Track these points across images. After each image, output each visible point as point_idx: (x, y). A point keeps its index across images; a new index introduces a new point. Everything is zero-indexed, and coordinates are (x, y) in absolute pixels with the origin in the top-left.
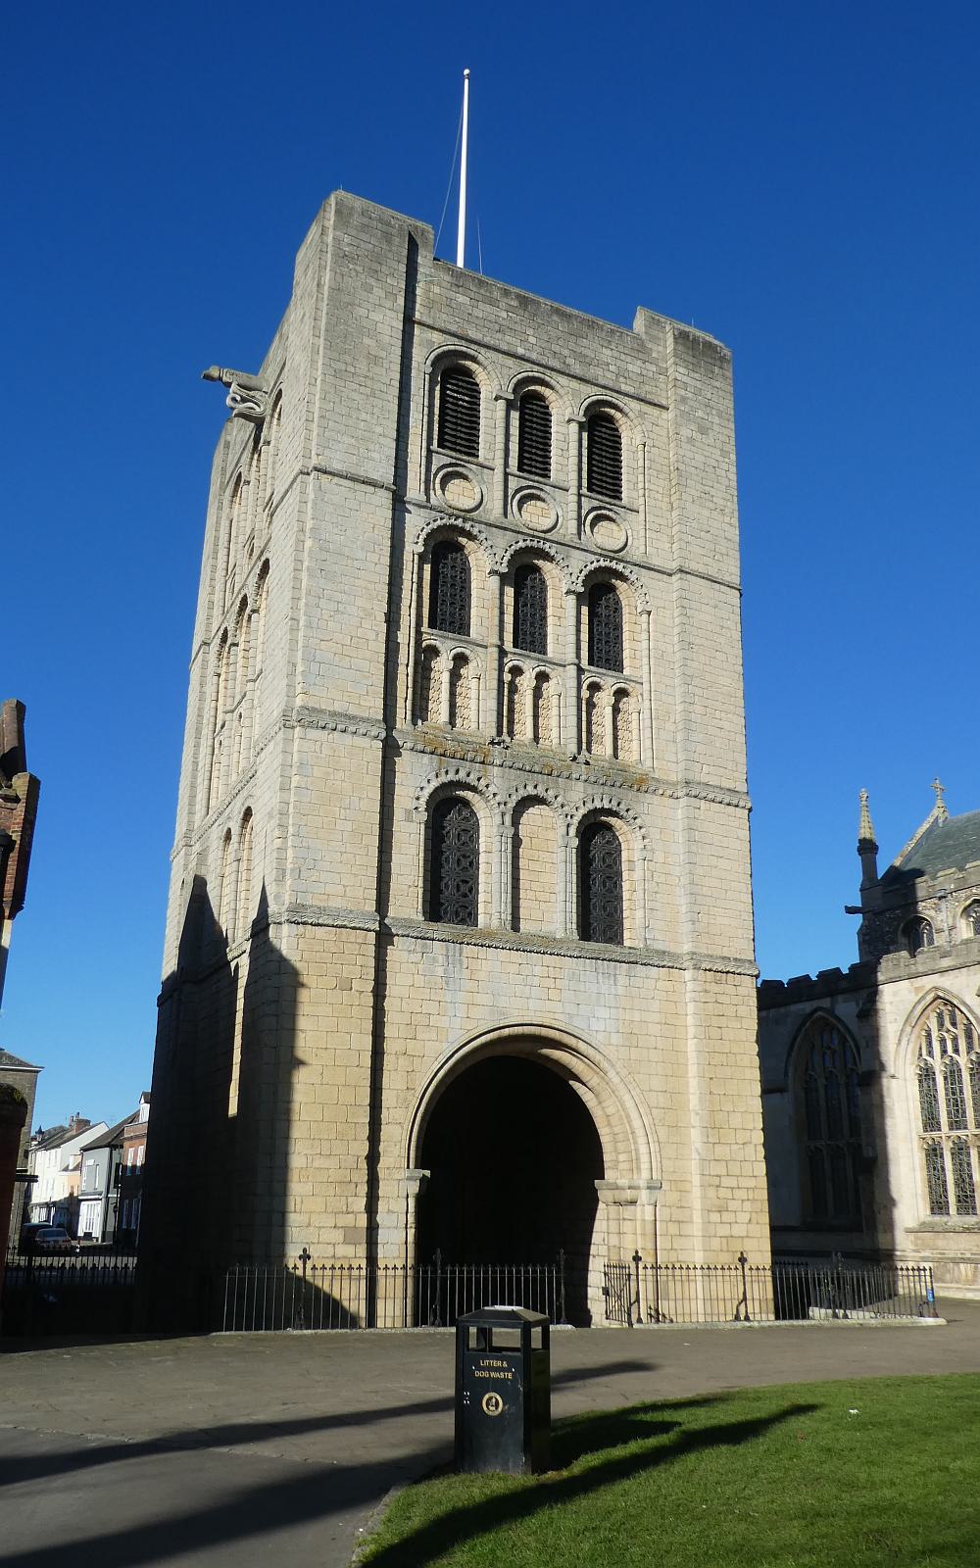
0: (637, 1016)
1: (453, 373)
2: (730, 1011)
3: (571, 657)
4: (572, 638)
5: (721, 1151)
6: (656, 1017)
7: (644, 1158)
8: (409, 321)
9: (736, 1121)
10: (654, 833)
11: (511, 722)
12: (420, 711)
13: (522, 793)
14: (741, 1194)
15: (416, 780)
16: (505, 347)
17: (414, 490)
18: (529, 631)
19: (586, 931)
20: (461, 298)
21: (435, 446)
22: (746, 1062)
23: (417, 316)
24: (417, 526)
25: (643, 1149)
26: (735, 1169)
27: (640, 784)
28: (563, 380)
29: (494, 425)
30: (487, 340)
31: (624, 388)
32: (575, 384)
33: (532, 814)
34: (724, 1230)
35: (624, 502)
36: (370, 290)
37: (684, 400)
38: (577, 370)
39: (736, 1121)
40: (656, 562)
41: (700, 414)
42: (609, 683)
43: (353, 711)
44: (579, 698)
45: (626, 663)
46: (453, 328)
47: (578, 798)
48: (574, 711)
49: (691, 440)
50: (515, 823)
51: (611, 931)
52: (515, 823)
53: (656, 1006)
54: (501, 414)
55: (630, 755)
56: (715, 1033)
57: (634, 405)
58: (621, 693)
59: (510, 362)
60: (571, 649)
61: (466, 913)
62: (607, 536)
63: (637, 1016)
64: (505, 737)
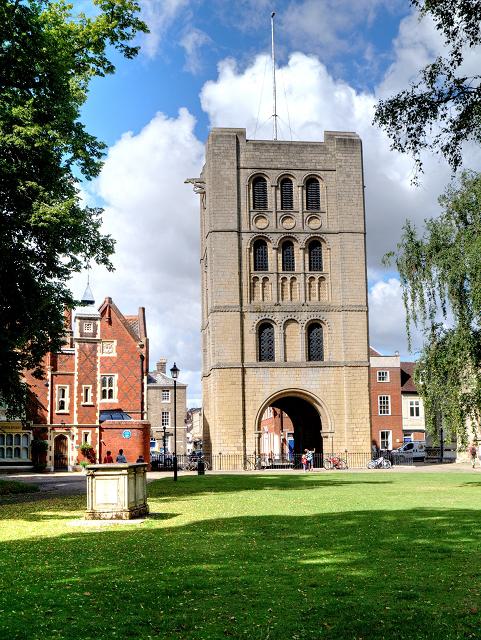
1: (258, 181)
3: (302, 270)
4: (302, 264)
5: (354, 421)
8: (238, 168)
9: (359, 411)
10: (332, 327)
11: (283, 295)
12: (252, 297)
13: (287, 319)
15: (251, 322)
16: (273, 167)
17: (245, 228)
18: (288, 264)
19: (310, 358)
20: (257, 153)
21: (252, 208)
23: (242, 165)
24: (247, 239)
27: (329, 309)
29: (273, 196)
30: (268, 166)
31: (318, 167)
32: (299, 172)
33: (292, 326)
35: (322, 210)
37: (340, 166)
40: (333, 230)
41: (348, 170)
42: (317, 276)
43: (230, 304)
44: (305, 284)
46: (254, 165)
47: (305, 318)
48: (303, 288)
49: (344, 181)
50: (284, 328)
51: (320, 357)
52: (284, 328)
54: (273, 191)
55: (324, 299)
58: (322, 279)
60: (302, 268)
61: (271, 358)
62: (314, 224)
64: (280, 302)
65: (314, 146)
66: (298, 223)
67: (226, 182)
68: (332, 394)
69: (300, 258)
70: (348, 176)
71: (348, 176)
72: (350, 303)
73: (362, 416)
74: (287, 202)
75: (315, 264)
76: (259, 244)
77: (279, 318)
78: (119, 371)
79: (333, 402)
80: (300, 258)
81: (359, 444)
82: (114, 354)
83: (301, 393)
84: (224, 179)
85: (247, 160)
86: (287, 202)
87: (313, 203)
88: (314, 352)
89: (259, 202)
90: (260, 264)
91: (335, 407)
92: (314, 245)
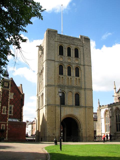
0: (81, 113)
2: (90, 112)
6: (82, 113)
7: (82, 127)
14: (91, 130)
18: (69, 74)
25: (81, 126)
26: (90, 128)
28: (72, 45)
32: (73, 46)
34: (89, 134)
36: (51, 39)
38: (73, 44)
39: (91, 123)
42: (78, 78)
45: (80, 76)
56: (89, 114)
57: (79, 47)
59: (66, 44)
63: (81, 113)
65: (77, 39)
66: (65, 59)
67: (51, 45)
69: (73, 72)
70: (87, 49)
71: (87, 49)
72: (88, 88)
74: (69, 54)
75: (77, 75)
76: (61, 67)
77: (66, 90)
78: (14, 104)
79: (83, 119)
80: (73, 72)
81: (90, 134)
82: (13, 98)
83: (73, 116)
84: (51, 44)
85: (58, 39)
86: (69, 54)
87: (77, 55)
88: (77, 103)
89: (61, 53)
90: (61, 72)
91: (83, 121)
92: (77, 70)
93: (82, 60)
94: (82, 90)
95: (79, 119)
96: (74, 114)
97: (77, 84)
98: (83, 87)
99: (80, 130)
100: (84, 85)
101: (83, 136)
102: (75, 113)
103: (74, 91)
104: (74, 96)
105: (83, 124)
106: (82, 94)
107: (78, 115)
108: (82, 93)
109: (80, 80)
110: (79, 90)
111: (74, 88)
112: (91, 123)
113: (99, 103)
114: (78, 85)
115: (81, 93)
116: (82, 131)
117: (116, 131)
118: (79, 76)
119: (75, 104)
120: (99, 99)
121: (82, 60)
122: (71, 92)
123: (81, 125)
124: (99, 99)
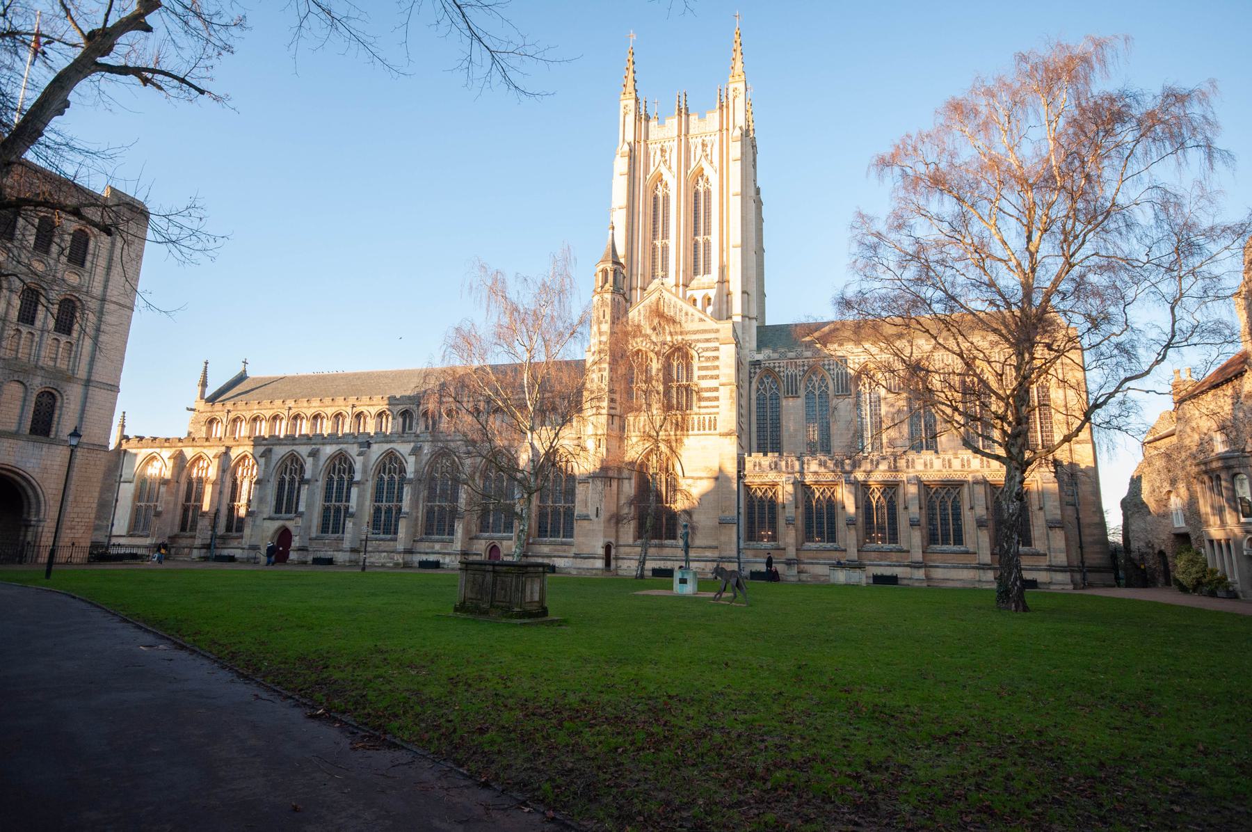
7: (43, 511)
22: (95, 480)
53: (59, 459)
68: (54, 476)
73: (86, 505)
79: (53, 486)
93: (100, 272)
94: (71, 385)
95: (35, 484)
96: (20, 465)
97: (55, 360)
98: (82, 373)
99: (31, 521)
100: (87, 367)
101: (42, 544)
102: (24, 460)
103: (38, 383)
104: (33, 399)
105: (51, 503)
106: (72, 398)
107: (37, 470)
108: (72, 395)
109: (74, 348)
110: (59, 382)
111: (39, 372)
112: (86, 500)
113: (123, 426)
114: (58, 365)
115: (65, 397)
116: (42, 524)
117: (176, 530)
118: (68, 332)
119: (31, 430)
120: (124, 413)
121: (100, 272)
122: (21, 383)
123: (43, 504)
124: (124, 413)
